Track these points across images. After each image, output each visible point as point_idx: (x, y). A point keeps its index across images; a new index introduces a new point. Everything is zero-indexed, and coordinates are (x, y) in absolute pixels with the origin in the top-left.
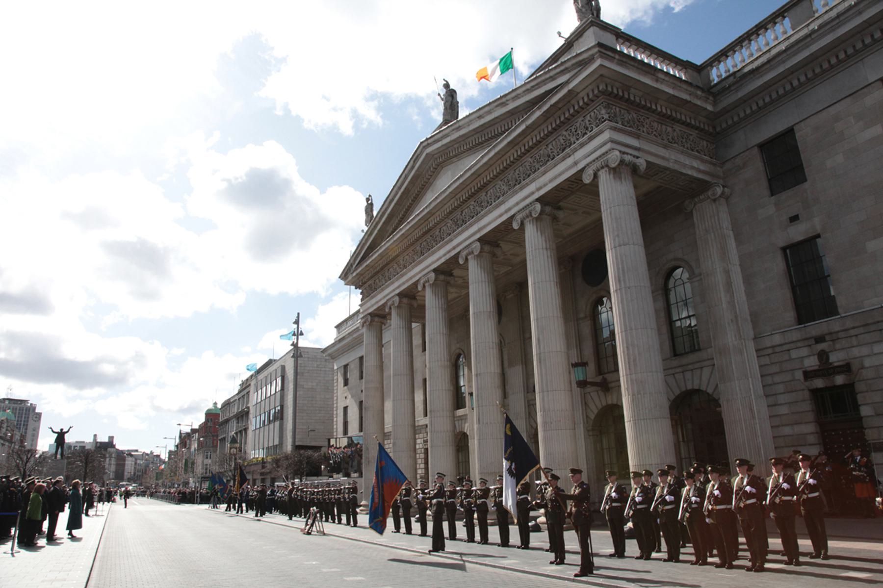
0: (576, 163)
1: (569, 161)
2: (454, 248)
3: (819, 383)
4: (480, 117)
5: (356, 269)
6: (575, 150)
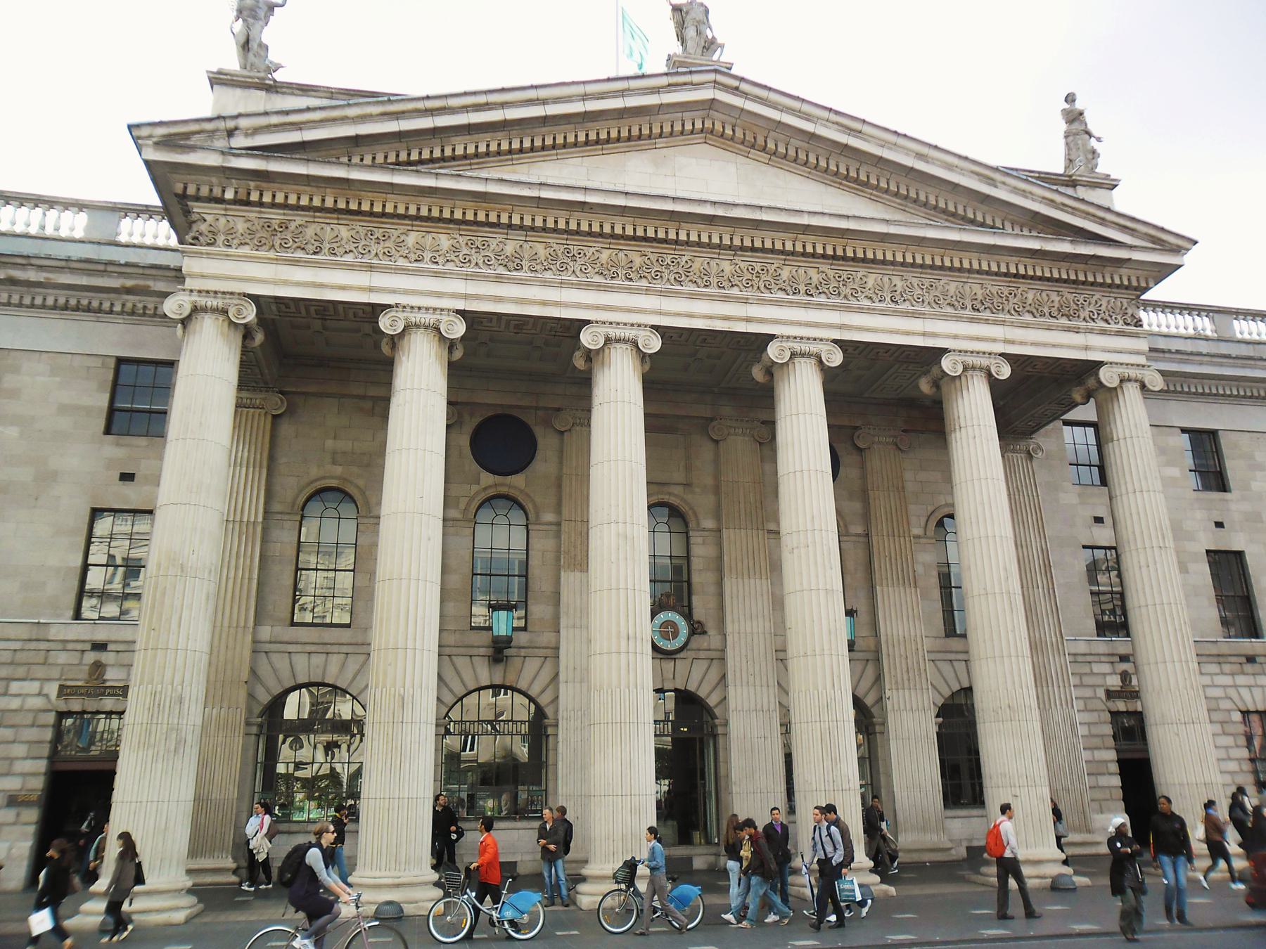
0: (1086, 348)
1: (1079, 339)
2: (748, 320)
3: (1121, 706)
4: (920, 156)
5: (253, 151)
6: (1091, 331)
